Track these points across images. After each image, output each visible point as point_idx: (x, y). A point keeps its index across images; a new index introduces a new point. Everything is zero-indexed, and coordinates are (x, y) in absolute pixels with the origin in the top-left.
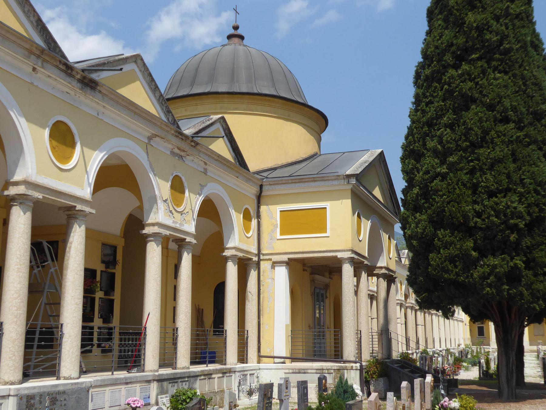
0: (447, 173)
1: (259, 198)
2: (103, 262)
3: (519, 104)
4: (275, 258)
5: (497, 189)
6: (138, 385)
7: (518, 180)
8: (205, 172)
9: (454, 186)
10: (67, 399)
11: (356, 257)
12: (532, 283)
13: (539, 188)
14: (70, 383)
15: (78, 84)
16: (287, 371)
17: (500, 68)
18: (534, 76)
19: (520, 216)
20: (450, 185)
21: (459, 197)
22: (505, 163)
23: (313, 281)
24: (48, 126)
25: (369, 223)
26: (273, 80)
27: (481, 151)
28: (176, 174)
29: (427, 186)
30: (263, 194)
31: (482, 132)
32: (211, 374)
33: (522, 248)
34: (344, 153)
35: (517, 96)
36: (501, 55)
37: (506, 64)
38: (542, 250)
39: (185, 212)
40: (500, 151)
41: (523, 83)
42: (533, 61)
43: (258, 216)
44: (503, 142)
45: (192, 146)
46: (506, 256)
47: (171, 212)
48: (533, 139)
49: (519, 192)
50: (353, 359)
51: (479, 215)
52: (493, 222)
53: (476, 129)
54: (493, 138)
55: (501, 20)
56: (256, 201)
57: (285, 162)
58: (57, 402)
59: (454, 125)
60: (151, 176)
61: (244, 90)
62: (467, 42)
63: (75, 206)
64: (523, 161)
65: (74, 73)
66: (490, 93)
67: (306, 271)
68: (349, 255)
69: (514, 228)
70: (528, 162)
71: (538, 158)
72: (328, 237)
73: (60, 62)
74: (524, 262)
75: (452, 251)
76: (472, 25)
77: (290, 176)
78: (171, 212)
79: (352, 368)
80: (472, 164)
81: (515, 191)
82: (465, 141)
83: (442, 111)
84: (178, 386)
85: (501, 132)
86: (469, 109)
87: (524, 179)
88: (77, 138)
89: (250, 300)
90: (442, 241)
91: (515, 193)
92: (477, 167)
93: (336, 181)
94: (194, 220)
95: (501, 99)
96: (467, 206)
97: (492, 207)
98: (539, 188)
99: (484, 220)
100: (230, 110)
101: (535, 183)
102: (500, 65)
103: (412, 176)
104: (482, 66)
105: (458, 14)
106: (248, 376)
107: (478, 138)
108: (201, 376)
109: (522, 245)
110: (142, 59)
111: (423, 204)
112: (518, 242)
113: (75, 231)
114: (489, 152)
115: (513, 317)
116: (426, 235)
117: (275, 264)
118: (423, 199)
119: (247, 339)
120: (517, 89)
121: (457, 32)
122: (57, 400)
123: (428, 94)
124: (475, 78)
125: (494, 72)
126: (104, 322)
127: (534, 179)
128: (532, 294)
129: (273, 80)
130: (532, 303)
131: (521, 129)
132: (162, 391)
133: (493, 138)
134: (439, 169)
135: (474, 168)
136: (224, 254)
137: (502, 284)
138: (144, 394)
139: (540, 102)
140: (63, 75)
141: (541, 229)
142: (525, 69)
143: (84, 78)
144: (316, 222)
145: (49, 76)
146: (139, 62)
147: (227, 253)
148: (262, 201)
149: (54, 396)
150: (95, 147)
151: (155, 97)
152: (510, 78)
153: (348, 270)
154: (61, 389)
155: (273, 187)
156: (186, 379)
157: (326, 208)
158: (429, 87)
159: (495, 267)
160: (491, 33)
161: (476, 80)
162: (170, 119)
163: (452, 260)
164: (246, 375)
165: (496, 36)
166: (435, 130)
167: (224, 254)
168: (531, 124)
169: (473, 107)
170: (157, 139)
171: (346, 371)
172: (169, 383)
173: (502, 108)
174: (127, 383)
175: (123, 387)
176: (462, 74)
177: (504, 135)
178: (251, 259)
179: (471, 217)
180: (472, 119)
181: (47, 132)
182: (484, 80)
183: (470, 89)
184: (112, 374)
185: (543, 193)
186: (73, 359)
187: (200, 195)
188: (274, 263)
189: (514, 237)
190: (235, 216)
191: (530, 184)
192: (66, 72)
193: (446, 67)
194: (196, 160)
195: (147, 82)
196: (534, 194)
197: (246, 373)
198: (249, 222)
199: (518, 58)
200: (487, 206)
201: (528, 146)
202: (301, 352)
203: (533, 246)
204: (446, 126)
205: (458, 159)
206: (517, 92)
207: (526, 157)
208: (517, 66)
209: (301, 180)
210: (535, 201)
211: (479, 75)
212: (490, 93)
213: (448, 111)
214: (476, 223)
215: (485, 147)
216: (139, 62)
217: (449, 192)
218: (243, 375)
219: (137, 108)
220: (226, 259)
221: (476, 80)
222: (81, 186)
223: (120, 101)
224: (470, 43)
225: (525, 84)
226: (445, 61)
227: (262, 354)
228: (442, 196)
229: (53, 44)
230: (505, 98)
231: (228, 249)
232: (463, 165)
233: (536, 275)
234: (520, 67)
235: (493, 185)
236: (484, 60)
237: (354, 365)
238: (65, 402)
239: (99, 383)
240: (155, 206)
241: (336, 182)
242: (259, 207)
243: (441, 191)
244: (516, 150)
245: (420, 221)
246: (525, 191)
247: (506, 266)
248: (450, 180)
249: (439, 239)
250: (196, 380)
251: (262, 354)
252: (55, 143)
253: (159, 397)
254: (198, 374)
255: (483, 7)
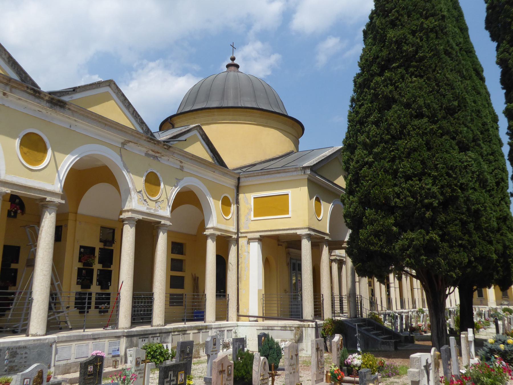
0: (373, 162)
1: (238, 189)
2: (101, 241)
3: (431, 102)
4: (250, 236)
5: (413, 173)
6: (107, 340)
7: (432, 165)
8: (182, 168)
9: (378, 172)
10: (28, 353)
11: (313, 233)
12: (448, 254)
13: (451, 172)
14: (32, 340)
15: (48, 104)
16: (258, 328)
17: (416, 73)
18: (447, 78)
19: (434, 196)
20: (375, 172)
21: (381, 181)
22: (420, 152)
23: (288, 253)
24: (19, 137)
25: (330, 206)
26: (255, 96)
27: (400, 142)
28: (151, 171)
29: (358, 173)
30: (241, 184)
31: (400, 127)
32: (186, 331)
33: (438, 224)
34: (313, 150)
35: (431, 95)
36: (416, 62)
37: (421, 69)
38: (456, 225)
39: (160, 200)
40: (415, 142)
41: (436, 84)
42: (446, 66)
43: (237, 202)
44: (418, 134)
45: (165, 148)
46: (423, 231)
47: (145, 200)
48: (446, 131)
49: (433, 176)
50: (311, 318)
51: (398, 196)
52: (409, 202)
53: (395, 124)
54: (409, 131)
55: (417, 34)
56: (235, 191)
57: (263, 159)
58: (17, 356)
59: (379, 122)
60: (125, 173)
61: (231, 104)
62: (389, 54)
63: (46, 198)
64: (437, 150)
65: (42, 95)
66: (406, 94)
67: (281, 245)
68: (306, 232)
69: (429, 206)
70: (441, 150)
71: (451, 146)
72: (290, 217)
73: (28, 87)
74: (439, 236)
75: (376, 227)
76: (392, 40)
77: (261, 170)
78: (145, 200)
79: (309, 326)
80: (393, 153)
81: (429, 175)
82: (387, 134)
83: (370, 111)
84: (149, 341)
85: (415, 126)
86: (391, 108)
87: (438, 164)
88: (48, 145)
89: (231, 269)
90: (369, 219)
91: (430, 176)
92: (397, 156)
93: (295, 172)
94: (169, 206)
95: (416, 98)
96: (388, 189)
97: (408, 190)
98: (451, 172)
99: (402, 200)
100: (219, 120)
101: (447, 167)
102: (416, 71)
103: (348, 165)
104: (401, 73)
105: (382, 32)
106: (226, 332)
107: (397, 131)
108: (174, 332)
109: (438, 221)
110: (115, 84)
111: (355, 188)
112: (433, 219)
113: (46, 218)
114: (407, 143)
115: (440, 283)
116: (357, 214)
117: (250, 240)
118: (355, 184)
119: (228, 301)
120: (431, 89)
121: (382, 47)
122: (18, 354)
123: (361, 98)
124: (395, 82)
125: (411, 77)
126: (102, 289)
127: (445, 164)
128: (449, 264)
129: (255, 96)
130: (450, 271)
131: (435, 122)
132: (131, 345)
133: (409, 131)
134: (366, 159)
135: (395, 157)
136: (205, 233)
137: (421, 255)
138: (113, 347)
139: (452, 99)
140: (31, 97)
141: (455, 206)
142: (438, 73)
143: (52, 99)
144: (280, 206)
145: (19, 99)
146: (113, 85)
147: (207, 232)
148: (241, 190)
149: (14, 350)
150: (66, 151)
151: (130, 112)
152: (424, 81)
153: (306, 246)
154: (23, 344)
155: (247, 178)
156: (158, 335)
157: (288, 194)
158: (362, 92)
159: (412, 240)
160: (408, 45)
161: (396, 84)
162: (144, 129)
163: (377, 234)
164: (223, 331)
165: (412, 47)
166: (365, 127)
167: (205, 233)
168: (444, 118)
169: (394, 106)
170: (131, 144)
171: (304, 329)
172: (140, 338)
173: (417, 106)
174: (95, 339)
175: (91, 342)
176: (385, 80)
177: (419, 128)
178: (231, 237)
179: (392, 198)
180: (392, 116)
181: (17, 142)
182: (403, 84)
183: (391, 92)
184: (84, 331)
185: (454, 176)
186: (40, 320)
187: (176, 187)
188: (249, 239)
189: (429, 214)
190: (213, 203)
191: (443, 168)
192: (34, 95)
193: (372, 76)
194: (171, 159)
195: (121, 101)
196: (446, 177)
197: (222, 329)
198: (228, 207)
199: (432, 64)
200: (404, 188)
201: (441, 137)
202: (276, 312)
203: (448, 222)
204: (373, 123)
205: (381, 150)
206: (431, 92)
207: (439, 146)
208: (430, 70)
209: (278, 171)
210: (448, 183)
211: (399, 79)
212: (406, 94)
213: (375, 111)
214: (396, 203)
215: (403, 139)
216: (113, 85)
217: (375, 178)
218: (220, 331)
219: (107, 121)
220: (206, 237)
221: (396, 84)
222: (52, 182)
223: (90, 116)
224: (392, 55)
225: (437, 85)
226: (373, 70)
227: (240, 314)
228: (367, 181)
229: (24, 75)
230: (419, 98)
231: (208, 229)
232: (386, 154)
233: (451, 247)
234: (434, 71)
235: (409, 170)
236: (403, 68)
237: (310, 323)
238: (26, 355)
239: (64, 339)
240: (129, 197)
241: (295, 173)
242: (238, 195)
243: (368, 177)
244: (430, 141)
245: (352, 202)
246: (438, 175)
247: (422, 239)
248: (375, 167)
249: (366, 218)
250: (169, 335)
251: (241, 313)
252: (25, 150)
253: (128, 350)
254: (170, 330)
255: (402, 25)
